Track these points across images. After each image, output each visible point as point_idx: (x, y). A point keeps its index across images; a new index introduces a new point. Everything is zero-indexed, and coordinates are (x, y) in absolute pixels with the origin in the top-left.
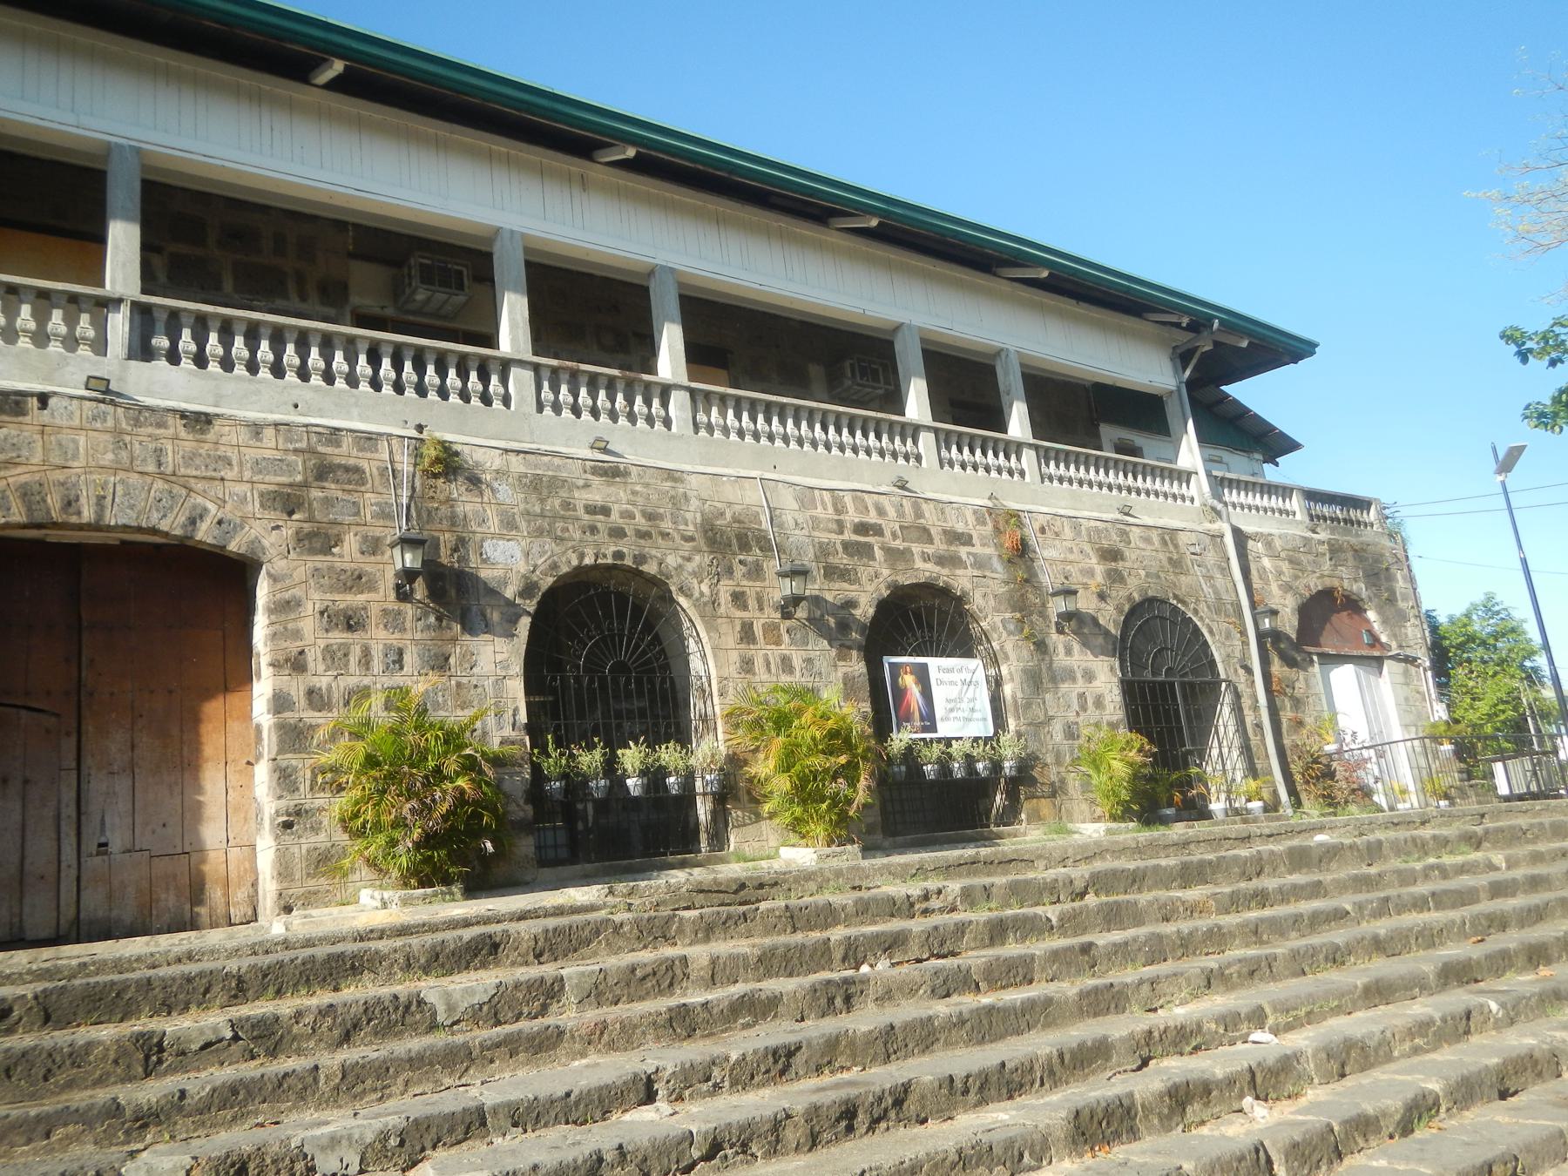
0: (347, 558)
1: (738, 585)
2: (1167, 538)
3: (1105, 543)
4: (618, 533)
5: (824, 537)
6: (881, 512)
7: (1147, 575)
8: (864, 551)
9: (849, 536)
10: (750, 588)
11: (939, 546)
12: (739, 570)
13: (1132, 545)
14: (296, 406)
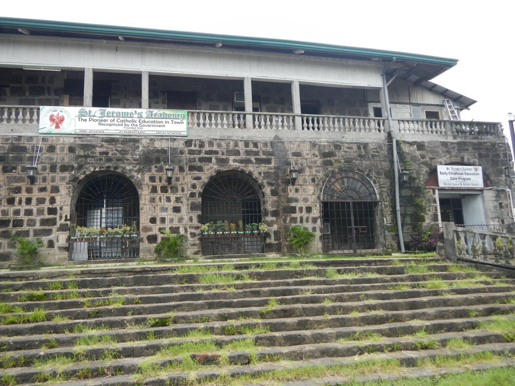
0: (17, 173)
1: (153, 174)
2: (362, 147)
3: (327, 151)
4: (109, 160)
5: (192, 156)
6: (219, 146)
7: (345, 162)
8: (209, 160)
9: (202, 155)
10: (157, 175)
11: (243, 156)
12: (154, 169)
13: (342, 150)
14: (12, 130)
